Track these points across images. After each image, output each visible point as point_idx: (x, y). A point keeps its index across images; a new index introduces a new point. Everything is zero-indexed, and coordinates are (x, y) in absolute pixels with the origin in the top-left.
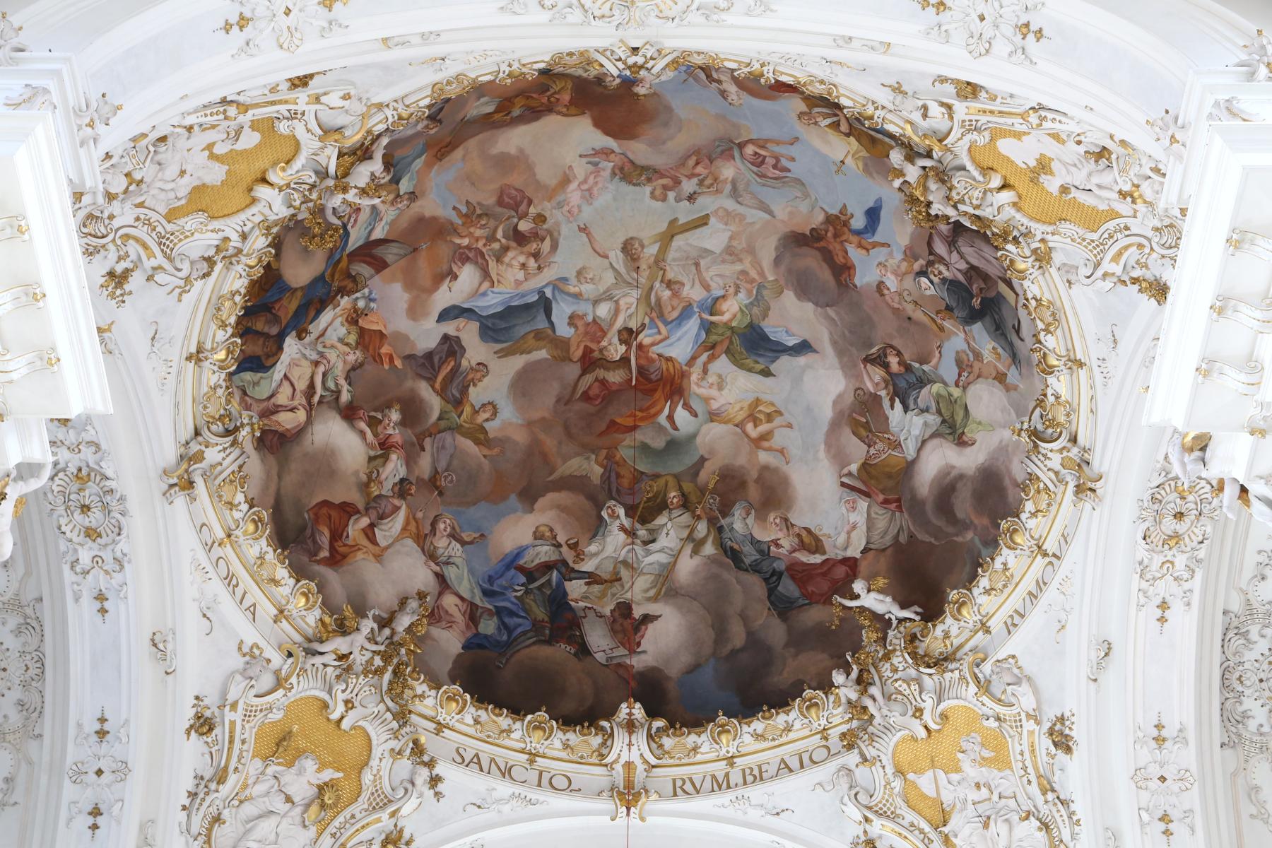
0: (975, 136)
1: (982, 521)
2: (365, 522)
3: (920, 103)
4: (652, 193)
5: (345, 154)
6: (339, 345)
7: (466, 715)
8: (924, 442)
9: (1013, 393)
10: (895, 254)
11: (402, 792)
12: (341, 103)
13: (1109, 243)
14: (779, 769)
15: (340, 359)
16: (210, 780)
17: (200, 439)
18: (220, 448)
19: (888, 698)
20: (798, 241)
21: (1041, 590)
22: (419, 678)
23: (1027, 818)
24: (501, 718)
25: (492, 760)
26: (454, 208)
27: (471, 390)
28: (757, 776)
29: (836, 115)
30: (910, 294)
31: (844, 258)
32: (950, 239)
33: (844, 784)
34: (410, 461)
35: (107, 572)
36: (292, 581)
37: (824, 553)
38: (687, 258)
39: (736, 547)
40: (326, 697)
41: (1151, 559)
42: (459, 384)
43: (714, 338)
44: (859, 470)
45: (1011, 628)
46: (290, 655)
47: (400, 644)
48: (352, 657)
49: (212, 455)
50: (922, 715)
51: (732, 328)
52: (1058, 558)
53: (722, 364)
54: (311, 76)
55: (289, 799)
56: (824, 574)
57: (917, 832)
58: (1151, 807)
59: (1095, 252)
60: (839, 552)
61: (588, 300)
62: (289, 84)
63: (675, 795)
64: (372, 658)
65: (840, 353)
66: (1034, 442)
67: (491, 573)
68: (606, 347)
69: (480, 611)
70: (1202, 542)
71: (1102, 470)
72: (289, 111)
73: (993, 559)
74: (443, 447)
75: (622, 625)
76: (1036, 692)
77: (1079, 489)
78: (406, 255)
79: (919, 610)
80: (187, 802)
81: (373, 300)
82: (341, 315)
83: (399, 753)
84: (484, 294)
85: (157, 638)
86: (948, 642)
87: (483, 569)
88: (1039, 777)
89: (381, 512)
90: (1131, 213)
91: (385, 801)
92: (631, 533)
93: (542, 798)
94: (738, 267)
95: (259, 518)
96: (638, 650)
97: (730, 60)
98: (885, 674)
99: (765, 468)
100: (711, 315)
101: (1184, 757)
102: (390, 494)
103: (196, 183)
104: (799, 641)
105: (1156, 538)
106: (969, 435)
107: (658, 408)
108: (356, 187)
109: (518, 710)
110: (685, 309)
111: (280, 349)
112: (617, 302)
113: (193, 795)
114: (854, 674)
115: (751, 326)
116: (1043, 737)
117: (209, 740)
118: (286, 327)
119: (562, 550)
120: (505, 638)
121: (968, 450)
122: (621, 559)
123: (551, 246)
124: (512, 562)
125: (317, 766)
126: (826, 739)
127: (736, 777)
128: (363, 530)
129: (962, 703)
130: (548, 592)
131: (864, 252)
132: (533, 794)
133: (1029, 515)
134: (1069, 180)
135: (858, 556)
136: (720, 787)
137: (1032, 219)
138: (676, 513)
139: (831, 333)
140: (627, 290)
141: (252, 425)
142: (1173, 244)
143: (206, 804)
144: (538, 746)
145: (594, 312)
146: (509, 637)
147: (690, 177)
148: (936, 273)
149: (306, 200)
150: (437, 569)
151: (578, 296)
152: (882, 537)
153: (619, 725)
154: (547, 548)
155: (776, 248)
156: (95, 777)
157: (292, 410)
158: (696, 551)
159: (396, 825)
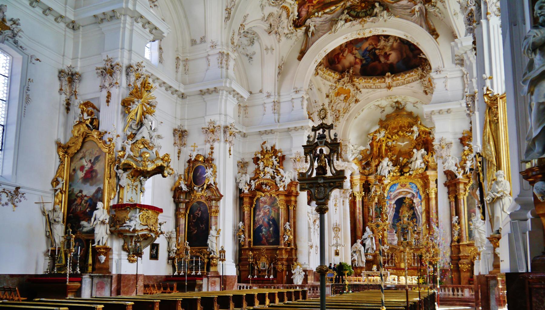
2: (342, 54)
28: (409, 82)
33: (421, 83)
87: (361, 53)
92: (385, 40)
124: (366, 50)
132: (375, 90)
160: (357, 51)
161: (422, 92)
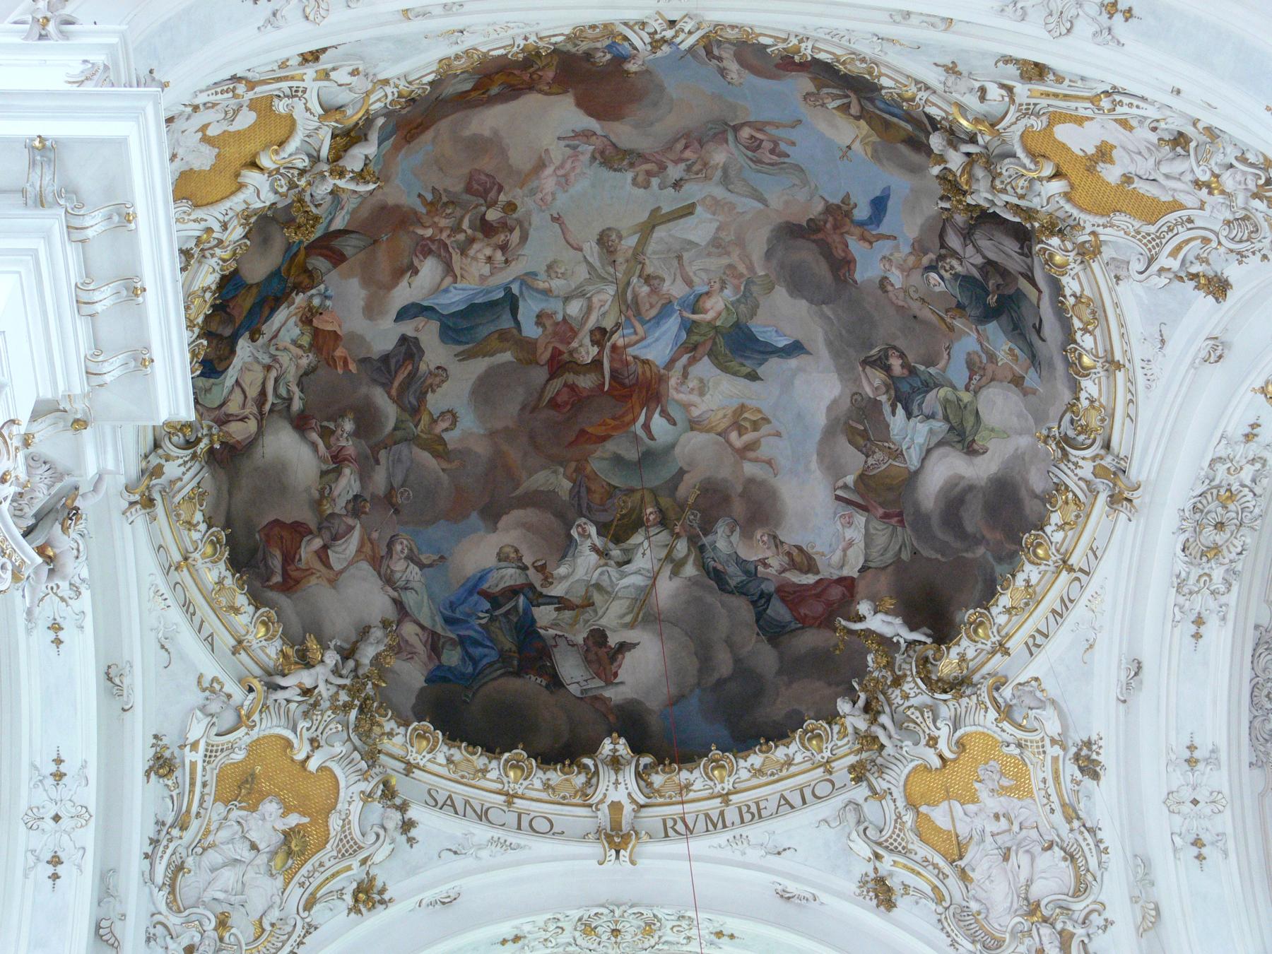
0: (1033, 121)
1: (994, 536)
2: (317, 543)
3: (977, 85)
4: (634, 179)
5: (337, 135)
6: (292, 348)
7: (438, 754)
8: (929, 451)
9: (1030, 396)
10: (901, 248)
11: (373, 838)
12: (348, 79)
13: (1168, 237)
14: (779, 806)
15: (293, 362)
16: (172, 826)
17: (160, 451)
18: (180, 461)
19: (899, 726)
20: (792, 232)
21: (1067, 609)
22: (386, 716)
23: (1050, 847)
24: (475, 757)
25: (467, 802)
26: (420, 195)
27: (430, 396)
28: (756, 814)
29: (847, 96)
30: (916, 291)
31: (844, 251)
32: (966, 231)
33: (851, 817)
34: (364, 476)
35: (62, 599)
36: (251, 609)
37: (818, 572)
38: (669, 251)
39: (720, 567)
40: (290, 735)
41: (1188, 573)
42: (416, 391)
43: (695, 338)
44: (856, 482)
45: (1033, 649)
46: (251, 690)
47: (368, 677)
48: (316, 691)
49: (172, 470)
50: (936, 743)
51: (716, 328)
52: (1087, 574)
53: (705, 367)
54: (324, 50)
55: (254, 847)
56: (818, 596)
57: (931, 868)
58: (1183, 831)
59: (1150, 246)
60: (832, 571)
61: (557, 297)
62: (300, 59)
63: (667, 836)
64: (337, 693)
65: (836, 354)
66: (1063, 449)
67: (453, 598)
68: (576, 350)
69: (442, 640)
70: (1240, 553)
71: (1140, 479)
72: (290, 88)
73: (1014, 576)
74: (399, 460)
75: (596, 654)
76: (1062, 716)
77: (1115, 500)
78: (365, 247)
79: (929, 631)
80: (149, 850)
81: (326, 297)
82: (296, 314)
83: (369, 796)
84: (446, 291)
85: (113, 672)
86: (964, 665)
88: (1063, 805)
89: (334, 532)
90: (1198, 204)
91: (355, 847)
92: (603, 554)
93: (522, 843)
94: (725, 261)
95: (217, 539)
96: (616, 681)
97: (766, 35)
98: (895, 701)
99: (751, 481)
100: (694, 313)
101: (1216, 779)
102: (343, 512)
103: (186, 168)
104: (793, 668)
105: (1194, 550)
106: (980, 443)
107: (630, 417)
108: (353, 171)
109: (492, 749)
110: (664, 306)
111: (233, 352)
112: (589, 299)
113: (155, 842)
114: (861, 703)
115: (737, 325)
116: (1068, 762)
117: (170, 783)
118: (239, 329)
119: (528, 572)
120: (470, 670)
121: (979, 460)
122: (593, 582)
123: (520, 238)
124: (475, 587)
125: (282, 811)
126: (831, 773)
127: (731, 815)
128: (316, 552)
129: (980, 729)
130: (515, 620)
131: (866, 245)
132: (513, 838)
133: (1055, 528)
134: (1132, 169)
135: (856, 575)
136: (715, 826)
137: (1082, 209)
138: (653, 531)
139: (826, 333)
140: (601, 286)
141: (211, 435)
142: (1245, 238)
143: (169, 852)
144: (517, 787)
145: (564, 309)
146: (475, 669)
147: (676, 162)
148: (948, 267)
149: (292, 185)
150: (395, 594)
151: (547, 293)
152: (882, 555)
153: (603, 761)
154: (513, 570)
155: (769, 240)
156: (52, 823)
157: (243, 419)
158: (675, 573)
159: (368, 873)
160: (414, 572)
161: (853, 887)
